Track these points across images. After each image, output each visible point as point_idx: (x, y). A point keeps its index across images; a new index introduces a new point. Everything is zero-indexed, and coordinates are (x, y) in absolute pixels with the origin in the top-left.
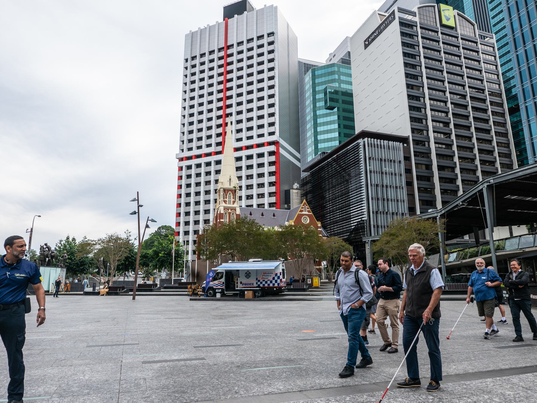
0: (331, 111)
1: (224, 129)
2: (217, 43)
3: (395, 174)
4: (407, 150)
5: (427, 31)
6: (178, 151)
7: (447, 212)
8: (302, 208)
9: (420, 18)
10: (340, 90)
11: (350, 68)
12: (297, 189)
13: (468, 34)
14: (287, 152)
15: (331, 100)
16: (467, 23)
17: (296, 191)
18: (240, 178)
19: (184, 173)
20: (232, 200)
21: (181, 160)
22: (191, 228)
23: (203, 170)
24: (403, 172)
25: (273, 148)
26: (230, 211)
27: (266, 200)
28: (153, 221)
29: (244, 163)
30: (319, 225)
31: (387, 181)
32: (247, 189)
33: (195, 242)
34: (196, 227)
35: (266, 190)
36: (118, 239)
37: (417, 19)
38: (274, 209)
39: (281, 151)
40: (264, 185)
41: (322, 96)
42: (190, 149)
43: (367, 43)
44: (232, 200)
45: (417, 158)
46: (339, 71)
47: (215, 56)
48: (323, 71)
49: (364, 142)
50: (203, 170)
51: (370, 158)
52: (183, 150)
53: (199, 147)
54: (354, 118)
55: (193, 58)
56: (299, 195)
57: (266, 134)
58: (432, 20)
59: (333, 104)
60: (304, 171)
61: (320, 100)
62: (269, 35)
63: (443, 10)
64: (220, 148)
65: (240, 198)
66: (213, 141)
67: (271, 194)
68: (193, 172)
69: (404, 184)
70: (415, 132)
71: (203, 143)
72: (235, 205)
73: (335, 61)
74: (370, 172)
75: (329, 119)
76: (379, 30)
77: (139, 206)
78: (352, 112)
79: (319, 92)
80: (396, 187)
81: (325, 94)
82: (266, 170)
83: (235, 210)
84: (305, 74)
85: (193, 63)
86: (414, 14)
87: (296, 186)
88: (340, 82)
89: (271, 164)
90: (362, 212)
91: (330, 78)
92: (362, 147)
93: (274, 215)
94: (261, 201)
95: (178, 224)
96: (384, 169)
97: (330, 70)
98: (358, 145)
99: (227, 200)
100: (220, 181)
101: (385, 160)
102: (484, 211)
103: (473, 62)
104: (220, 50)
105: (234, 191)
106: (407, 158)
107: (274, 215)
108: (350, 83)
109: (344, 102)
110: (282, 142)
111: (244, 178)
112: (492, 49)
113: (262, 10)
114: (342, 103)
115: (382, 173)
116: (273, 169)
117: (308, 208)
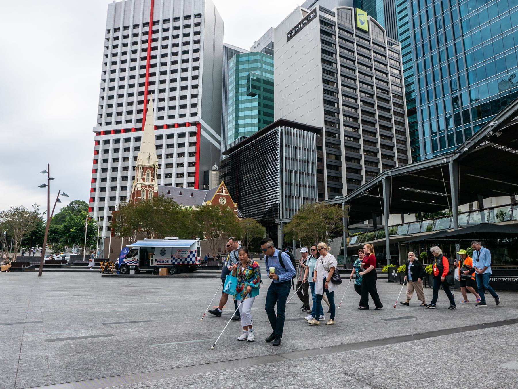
0: (253, 98)
1: (145, 106)
3: (308, 162)
4: (319, 140)
5: (344, 32)
6: (95, 124)
7: (351, 199)
8: (220, 189)
9: (338, 19)
10: (262, 78)
11: (273, 59)
12: (215, 170)
13: (379, 40)
14: (208, 133)
15: (254, 87)
16: (378, 29)
17: (215, 172)
18: (159, 156)
19: (101, 148)
20: (151, 178)
21: (99, 133)
22: (106, 204)
23: (121, 146)
24: (315, 160)
25: (194, 129)
26: (148, 188)
27: (185, 180)
28: (64, 195)
29: (164, 142)
30: (236, 206)
31: (300, 167)
32: (167, 168)
33: (109, 218)
34: (112, 204)
35: (186, 170)
36: (24, 212)
37: (335, 19)
38: (193, 188)
39: (203, 132)
40: (184, 165)
41: (243, 82)
42: (108, 124)
43: (289, 36)
44: (151, 178)
45: (328, 148)
46: (262, 60)
47: (139, 30)
48: (247, 58)
49: (282, 130)
50: (121, 146)
51: (286, 146)
52: (100, 124)
54: (273, 107)
55: (116, 30)
56: (218, 176)
58: (348, 22)
59: (255, 91)
60: (224, 153)
61: (242, 86)
62: (196, 16)
63: (359, 14)
64: (140, 125)
65: (159, 176)
66: (134, 117)
67: (190, 174)
68: (111, 147)
69: (315, 172)
70: (328, 124)
71: (123, 118)
72: (153, 183)
73: (259, 49)
74: (286, 158)
75: (250, 105)
76: (301, 25)
77: (50, 179)
78: (272, 100)
79: (242, 78)
80: (308, 174)
81: (248, 81)
82: (186, 150)
83: (153, 188)
84: (230, 59)
85: (116, 34)
86: (333, 14)
87: (215, 167)
89: (191, 144)
90: (276, 196)
91: (253, 65)
92: (279, 134)
93: (192, 195)
94: (179, 180)
95: (93, 199)
96: (298, 157)
97: (253, 58)
98: (276, 132)
99: (145, 177)
100: (138, 158)
101: (300, 148)
102: (382, 199)
103: (365, 68)
104: (145, 25)
105: (153, 169)
106: (320, 148)
107: (192, 195)
108: (272, 73)
109: (265, 90)
110: (204, 124)
111: (164, 156)
112: (397, 55)
114: (262, 90)
115: (296, 160)
116: (193, 149)
117: (225, 190)
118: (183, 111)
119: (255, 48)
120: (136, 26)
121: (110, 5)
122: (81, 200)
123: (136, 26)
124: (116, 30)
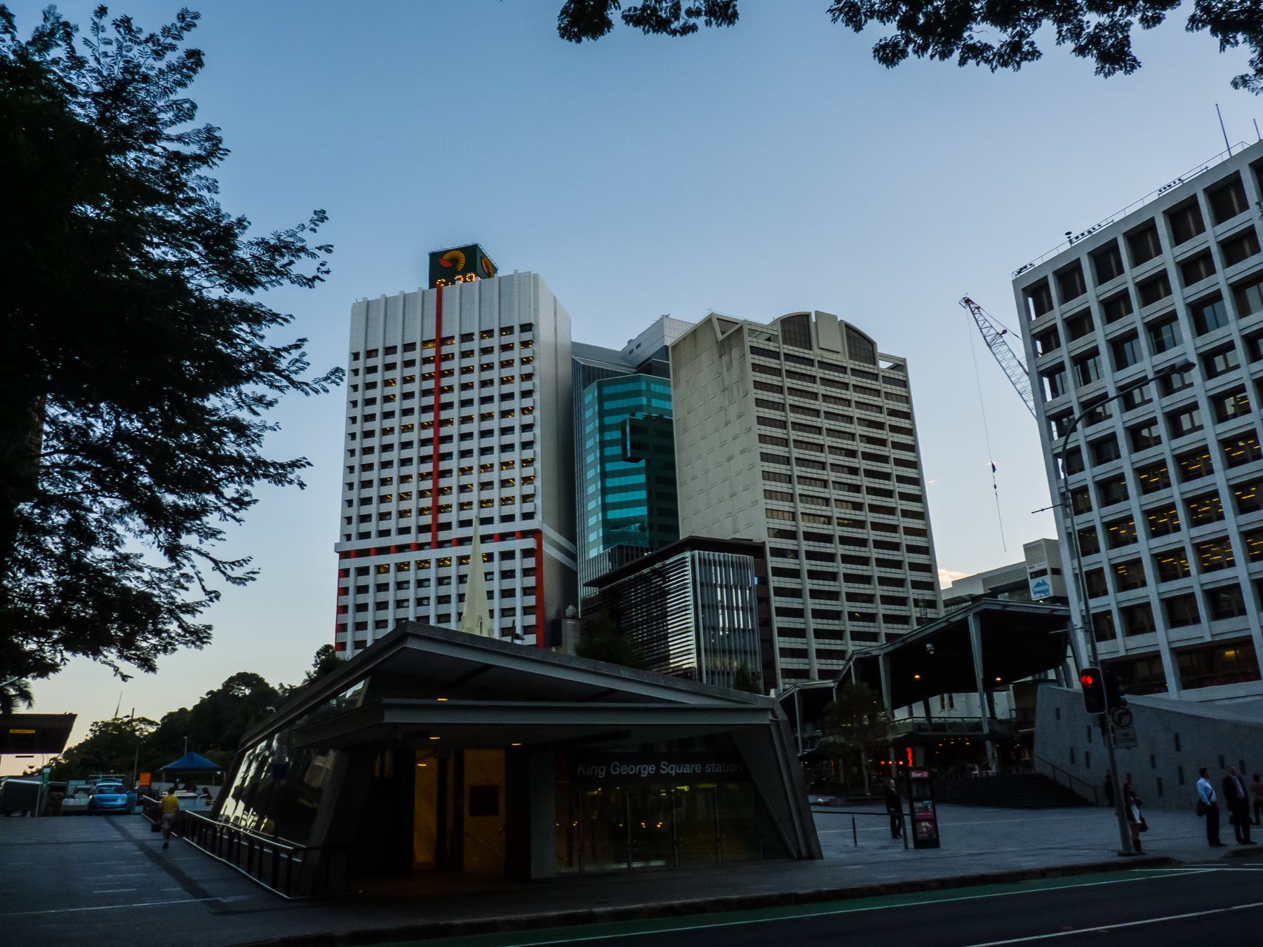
2: (419, 329)
25: (530, 543)
42: (365, 535)
46: (648, 389)
47: (416, 355)
49: (693, 557)
52: (348, 537)
53: (384, 533)
55: (371, 353)
60: (585, 585)
74: (703, 606)
78: (673, 498)
79: (612, 428)
84: (585, 387)
88: (651, 395)
104: (425, 343)
108: (668, 398)
113: (510, 278)
118: (507, 510)
119: (631, 352)
121: (356, 307)
122: (249, 672)
123: (409, 347)
124: (371, 353)
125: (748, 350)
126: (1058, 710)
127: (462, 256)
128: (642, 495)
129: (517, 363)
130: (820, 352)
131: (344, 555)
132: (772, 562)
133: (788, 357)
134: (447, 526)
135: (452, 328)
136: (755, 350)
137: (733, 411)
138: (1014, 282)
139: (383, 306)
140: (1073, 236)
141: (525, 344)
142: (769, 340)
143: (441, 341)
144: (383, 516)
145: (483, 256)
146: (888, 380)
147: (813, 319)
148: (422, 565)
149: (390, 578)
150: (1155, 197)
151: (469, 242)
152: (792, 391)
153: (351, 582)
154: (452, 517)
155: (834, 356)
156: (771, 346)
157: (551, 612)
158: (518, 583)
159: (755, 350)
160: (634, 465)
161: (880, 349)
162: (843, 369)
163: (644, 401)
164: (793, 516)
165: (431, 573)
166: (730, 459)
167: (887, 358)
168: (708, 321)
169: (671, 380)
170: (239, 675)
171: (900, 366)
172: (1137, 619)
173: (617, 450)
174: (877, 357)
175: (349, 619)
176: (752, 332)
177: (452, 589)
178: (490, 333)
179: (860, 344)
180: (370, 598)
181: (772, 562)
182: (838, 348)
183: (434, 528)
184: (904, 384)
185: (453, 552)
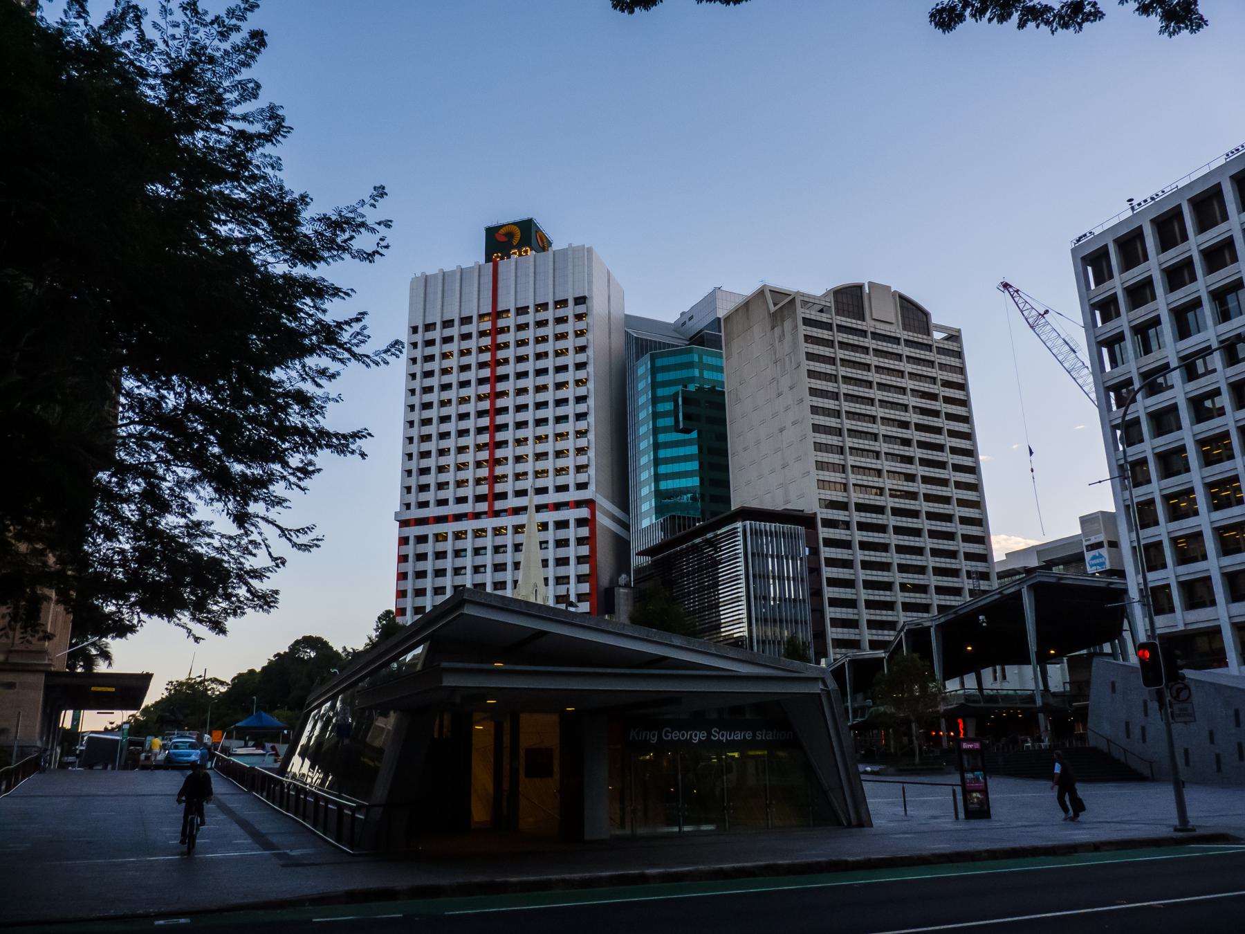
25: (584, 513)
42: (424, 505)
47: (472, 328)
49: (744, 527)
51: (753, 554)
52: (408, 506)
55: (429, 327)
57: (572, 487)
60: (639, 554)
74: (754, 576)
84: (638, 359)
88: (703, 367)
104: (481, 316)
108: (720, 369)
113: (564, 251)
118: (561, 480)
119: (684, 323)
120: (466, 320)
121: (414, 281)
123: (466, 320)
124: (429, 327)
125: (800, 322)
126: (1113, 684)
127: (517, 231)
128: (694, 466)
129: (571, 336)
130: (873, 323)
131: (404, 523)
132: (824, 533)
133: (841, 328)
134: (503, 496)
135: (507, 301)
136: (807, 322)
137: (785, 382)
138: (1073, 250)
139: (440, 278)
140: (1135, 203)
141: (579, 317)
142: (821, 311)
143: (497, 314)
144: (442, 486)
145: (538, 230)
146: (941, 351)
147: (867, 290)
148: (479, 533)
149: (448, 546)
150: (1222, 161)
151: (524, 217)
152: (844, 362)
153: (410, 550)
154: (508, 487)
155: (887, 327)
156: (824, 318)
157: (604, 580)
158: (572, 552)
159: (807, 322)
160: (687, 436)
161: (935, 320)
162: (896, 340)
163: (697, 373)
164: (845, 487)
165: (488, 541)
166: (781, 430)
167: (941, 328)
168: (761, 293)
169: (724, 351)
170: (304, 638)
171: (954, 336)
172: (1197, 594)
173: (669, 421)
174: (931, 328)
175: (409, 585)
176: (805, 303)
177: (508, 558)
178: (544, 306)
179: (914, 314)
180: (429, 565)
181: (824, 533)
182: (892, 319)
183: (490, 498)
184: (959, 355)
185: (508, 521)
